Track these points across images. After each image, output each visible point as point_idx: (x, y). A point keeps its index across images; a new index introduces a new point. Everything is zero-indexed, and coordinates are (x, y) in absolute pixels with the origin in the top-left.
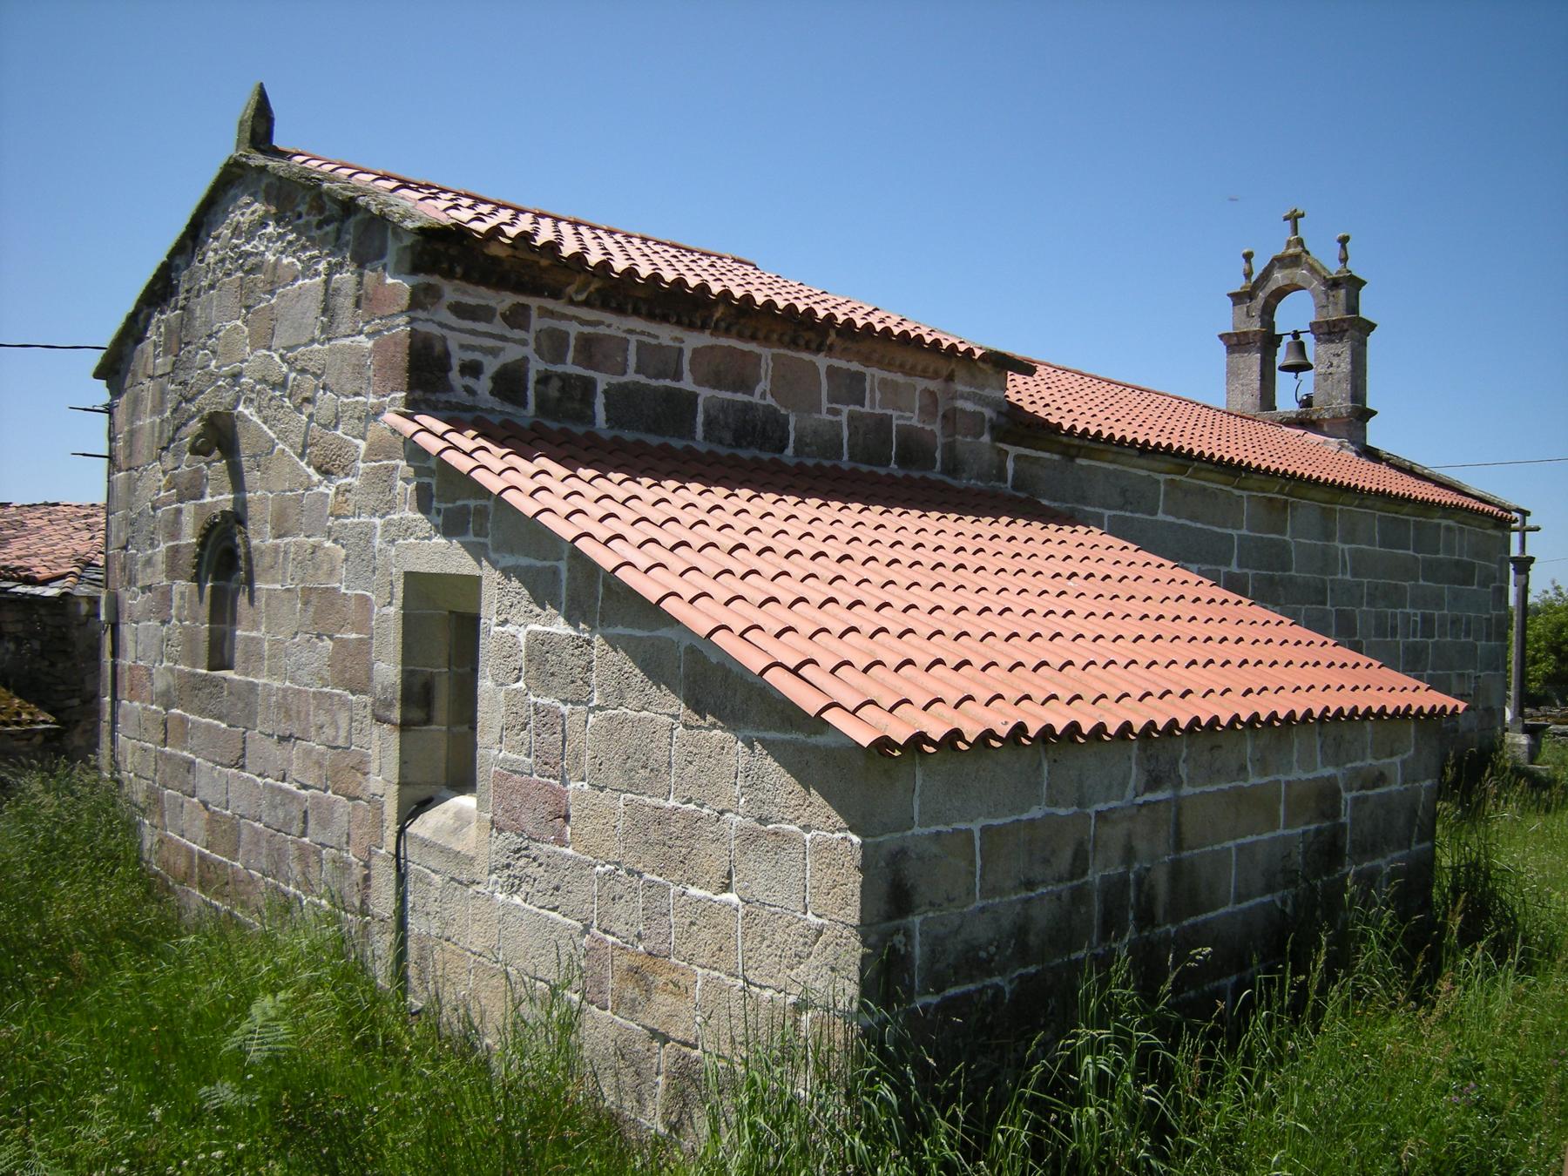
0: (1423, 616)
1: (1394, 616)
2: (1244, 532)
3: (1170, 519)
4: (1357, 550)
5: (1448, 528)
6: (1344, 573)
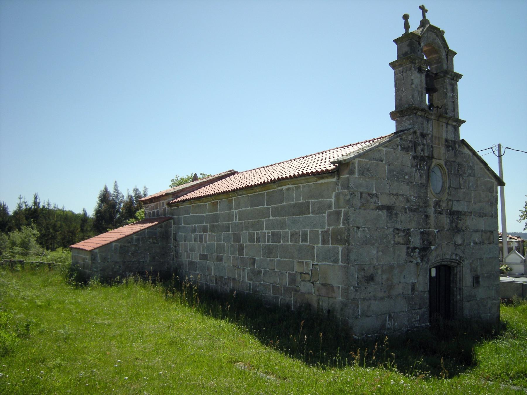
0: (273, 234)
1: (258, 234)
2: (207, 214)
3: (193, 214)
4: (240, 211)
5: (288, 189)
6: (236, 220)
